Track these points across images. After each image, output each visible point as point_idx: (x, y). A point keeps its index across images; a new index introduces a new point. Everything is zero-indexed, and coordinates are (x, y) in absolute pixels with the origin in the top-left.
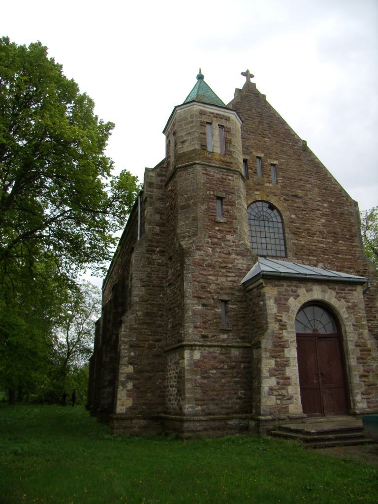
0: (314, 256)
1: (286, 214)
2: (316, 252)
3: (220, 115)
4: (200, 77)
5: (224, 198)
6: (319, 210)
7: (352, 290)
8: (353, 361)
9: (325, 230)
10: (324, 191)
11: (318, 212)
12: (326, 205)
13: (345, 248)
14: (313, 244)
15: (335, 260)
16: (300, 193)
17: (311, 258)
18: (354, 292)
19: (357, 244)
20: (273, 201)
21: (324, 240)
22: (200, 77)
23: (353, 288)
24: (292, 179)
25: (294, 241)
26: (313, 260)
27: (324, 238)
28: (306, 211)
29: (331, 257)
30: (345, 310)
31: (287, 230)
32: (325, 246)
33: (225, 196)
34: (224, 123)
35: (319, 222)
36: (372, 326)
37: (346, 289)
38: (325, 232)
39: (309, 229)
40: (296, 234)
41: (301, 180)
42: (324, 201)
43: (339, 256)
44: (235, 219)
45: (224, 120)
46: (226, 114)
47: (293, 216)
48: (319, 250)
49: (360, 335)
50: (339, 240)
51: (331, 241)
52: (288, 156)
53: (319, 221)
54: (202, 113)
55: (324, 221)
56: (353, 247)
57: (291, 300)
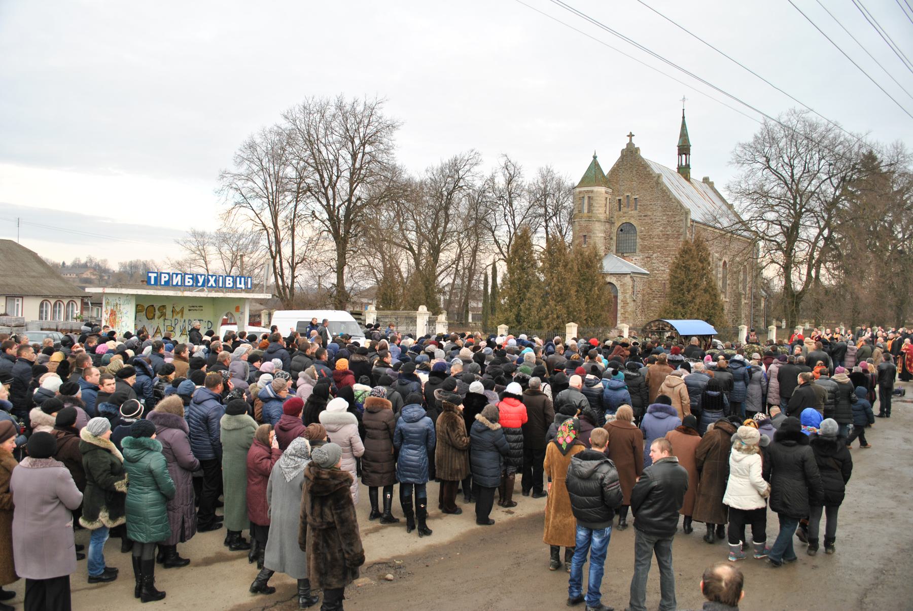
1: (638, 228)
4: (595, 157)
8: (619, 308)
16: (649, 213)
20: (632, 221)
22: (595, 157)
31: (638, 237)
34: (590, 195)
49: (625, 297)
54: (580, 192)
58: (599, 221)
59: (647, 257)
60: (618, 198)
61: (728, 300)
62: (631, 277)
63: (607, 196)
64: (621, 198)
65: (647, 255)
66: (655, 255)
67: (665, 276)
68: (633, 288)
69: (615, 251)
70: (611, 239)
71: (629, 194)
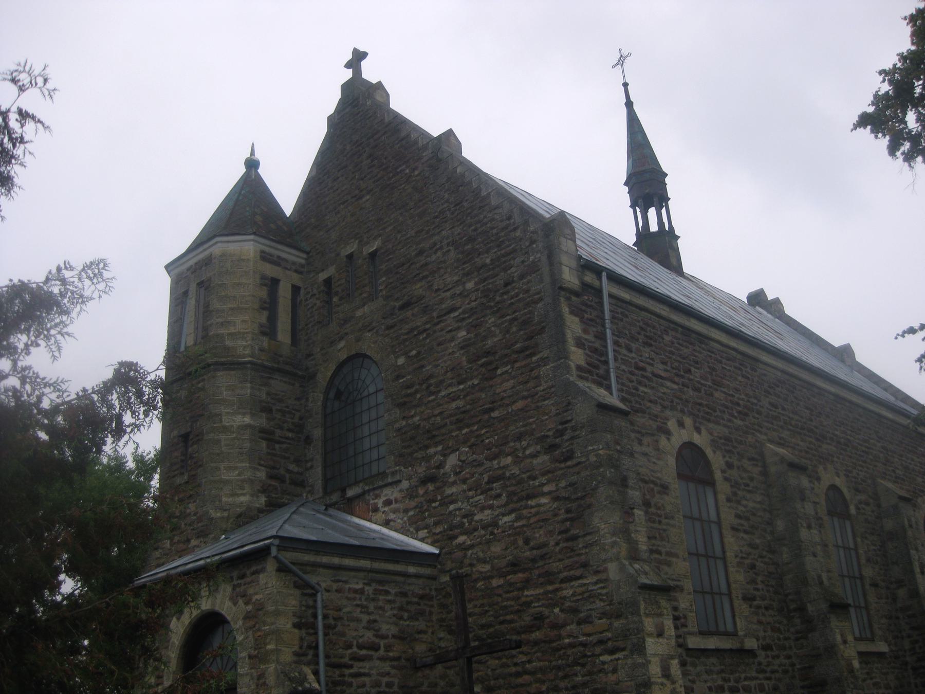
0: (436, 444)
2: (443, 431)
3: (199, 261)
4: (252, 164)
5: (190, 432)
6: (453, 309)
7: (256, 572)
9: (464, 358)
10: (470, 246)
11: (452, 315)
12: (470, 285)
13: (511, 383)
14: (436, 412)
15: (483, 432)
16: (418, 289)
17: (432, 451)
18: (261, 576)
19: (545, 353)
21: (461, 387)
22: (252, 164)
23: (259, 567)
24: (403, 264)
25: (397, 426)
26: (436, 453)
27: (459, 383)
28: (425, 330)
29: (475, 428)
30: (240, 623)
32: (460, 403)
33: (189, 430)
35: (453, 344)
36: (573, 595)
37: (248, 573)
38: (465, 363)
39: (431, 376)
40: (405, 403)
41: (421, 253)
42: (467, 274)
43: (495, 414)
44: (201, 466)
45: (203, 268)
46: (207, 253)
47: (401, 361)
48: (448, 421)
50: (496, 368)
51: (476, 382)
52: (400, 209)
53: (452, 339)
55: (464, 333)
56: (532, 370)
57: (174, 619)
58: (233, 365)
59: (424, 481)
60: (323, 276)
61: (883, 647)
62: (282, 569)
63: (271, 270)
64: (331, 271)
65: (421, 470)
66: (452, 460)
67: (496, 549)
68: (305, 624)
69: (319, 485)
70: (308, 440)
71: (351, 248)
